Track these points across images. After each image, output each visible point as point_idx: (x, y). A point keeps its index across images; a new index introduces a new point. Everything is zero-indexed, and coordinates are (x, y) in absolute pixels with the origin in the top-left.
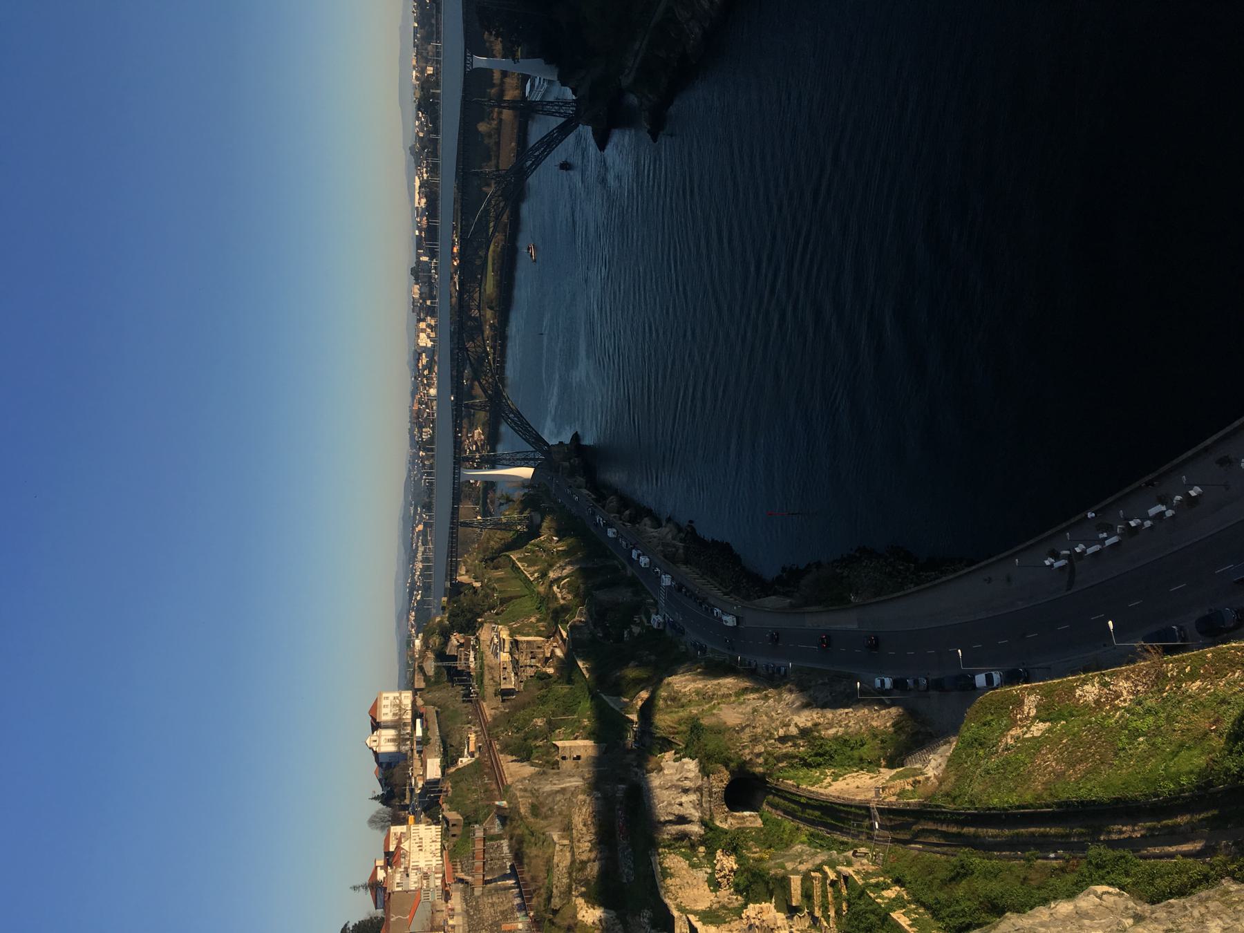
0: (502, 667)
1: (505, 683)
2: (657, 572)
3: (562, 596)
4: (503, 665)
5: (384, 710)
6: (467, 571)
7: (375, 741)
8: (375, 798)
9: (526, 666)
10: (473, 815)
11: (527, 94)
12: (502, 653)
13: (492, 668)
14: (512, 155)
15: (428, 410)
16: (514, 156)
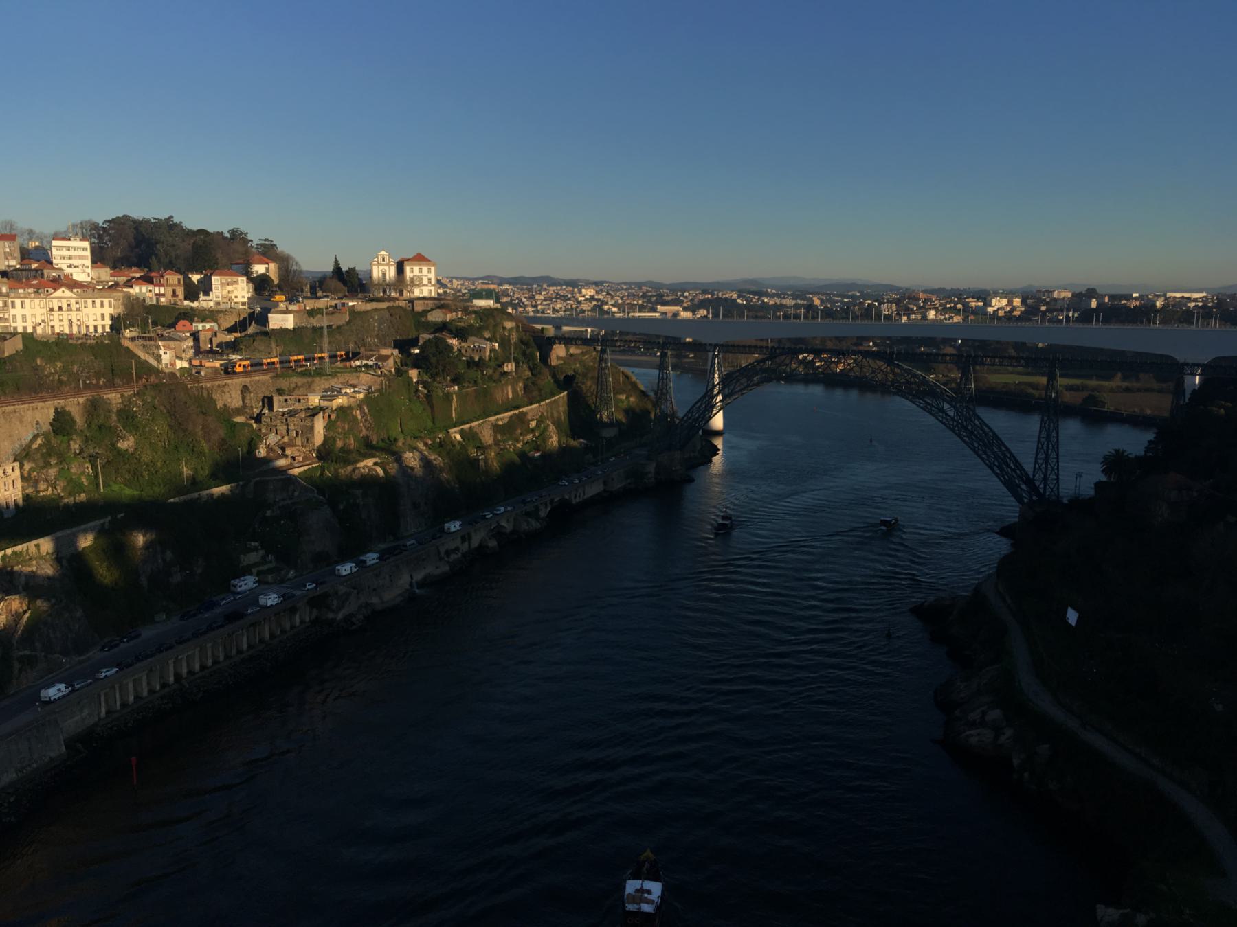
0: (301, 397)
1: (280, 401)
2: (305, 586)
3: (359, 468)
4: (304, 399)
5: (416, 269)
6: (571, 355)
7: (383, 260)
8: (336, 262)
9: (287, 425)
10: (7, 368)
11: (1046, 443)
12: (319, 397)
13: (310, 386)
14: (1136, 410)
15: (915, 309)
16: (1134, 412)
